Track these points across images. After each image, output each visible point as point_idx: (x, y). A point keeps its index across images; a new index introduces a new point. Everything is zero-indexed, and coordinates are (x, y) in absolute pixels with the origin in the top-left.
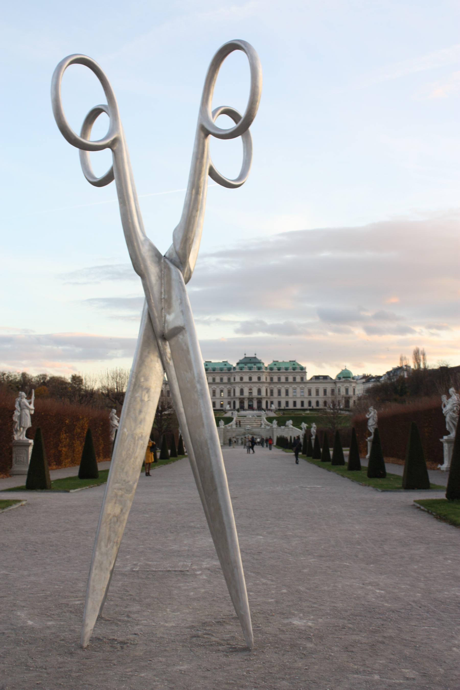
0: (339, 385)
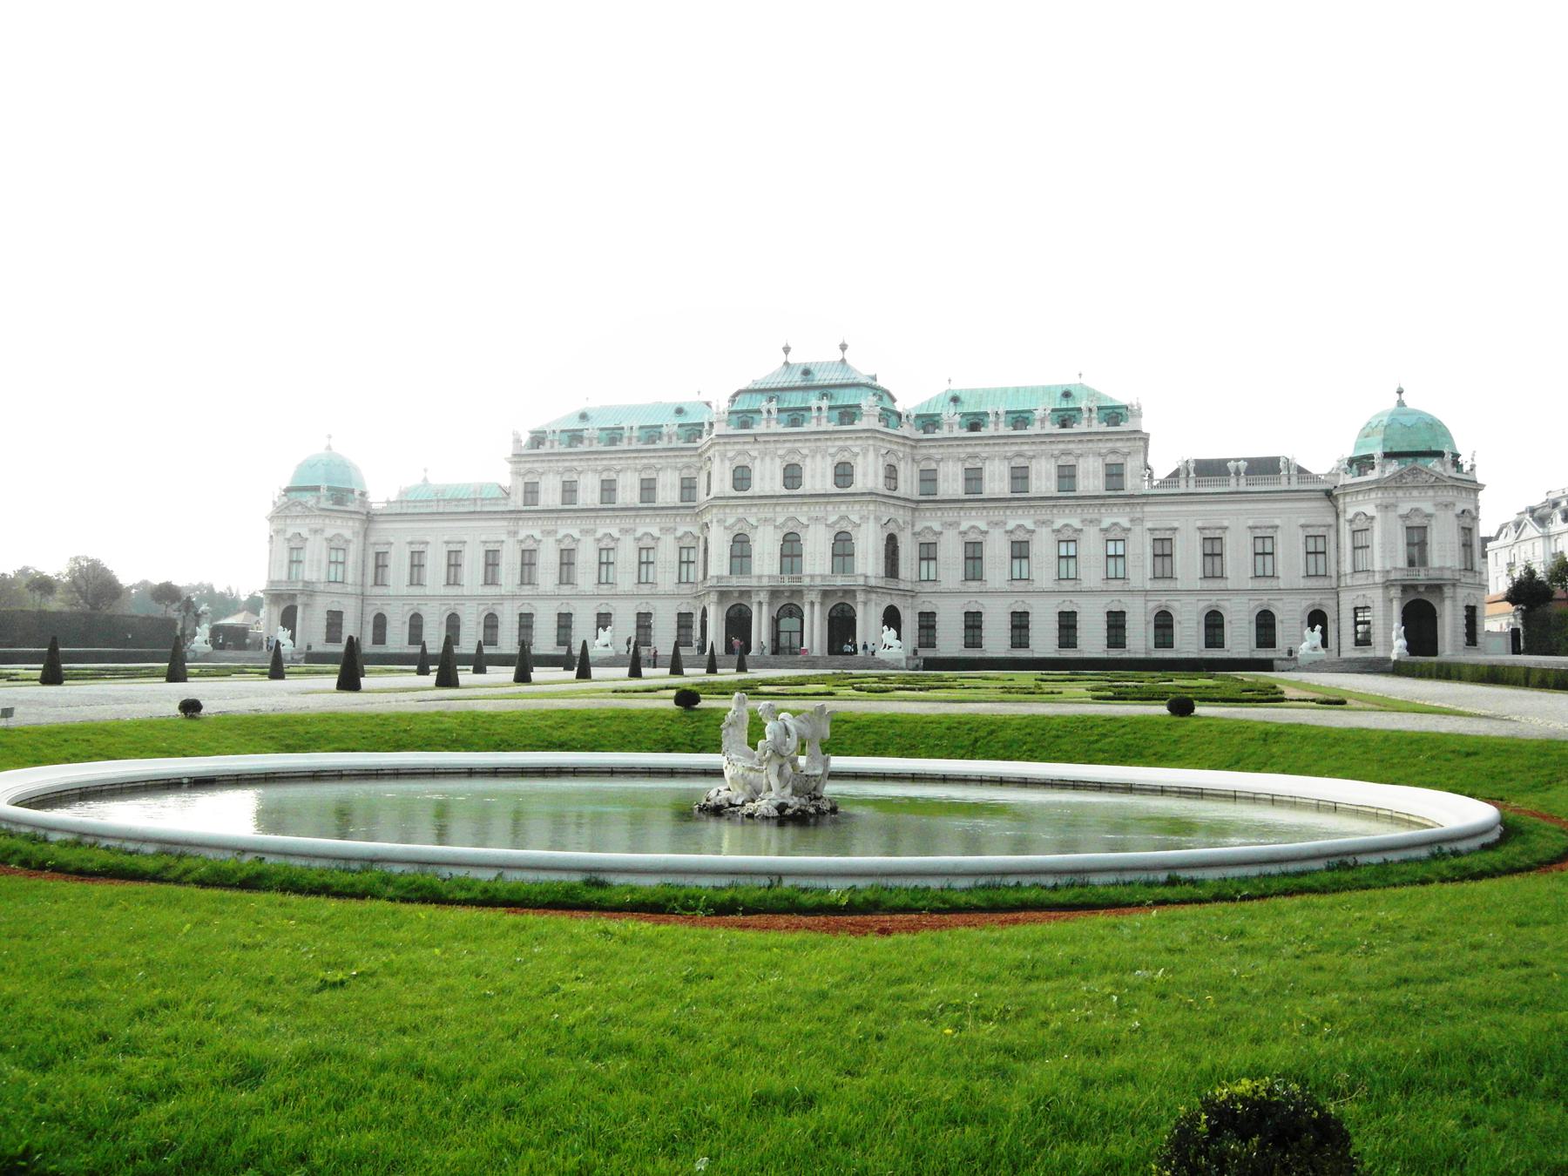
0: (1352, 507)
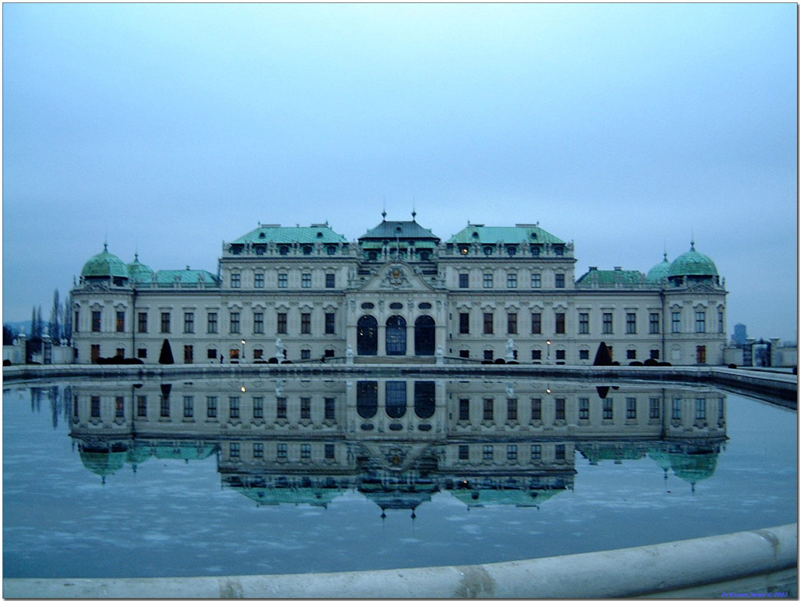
0: (672, 302)
